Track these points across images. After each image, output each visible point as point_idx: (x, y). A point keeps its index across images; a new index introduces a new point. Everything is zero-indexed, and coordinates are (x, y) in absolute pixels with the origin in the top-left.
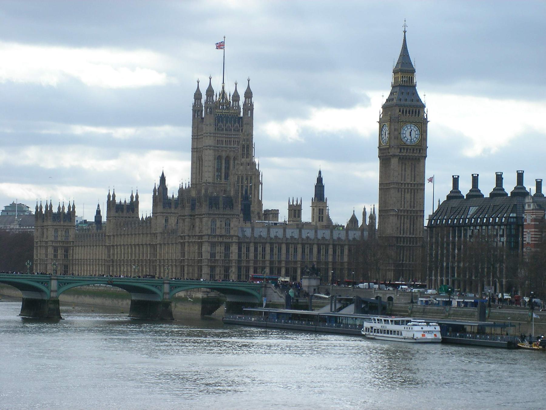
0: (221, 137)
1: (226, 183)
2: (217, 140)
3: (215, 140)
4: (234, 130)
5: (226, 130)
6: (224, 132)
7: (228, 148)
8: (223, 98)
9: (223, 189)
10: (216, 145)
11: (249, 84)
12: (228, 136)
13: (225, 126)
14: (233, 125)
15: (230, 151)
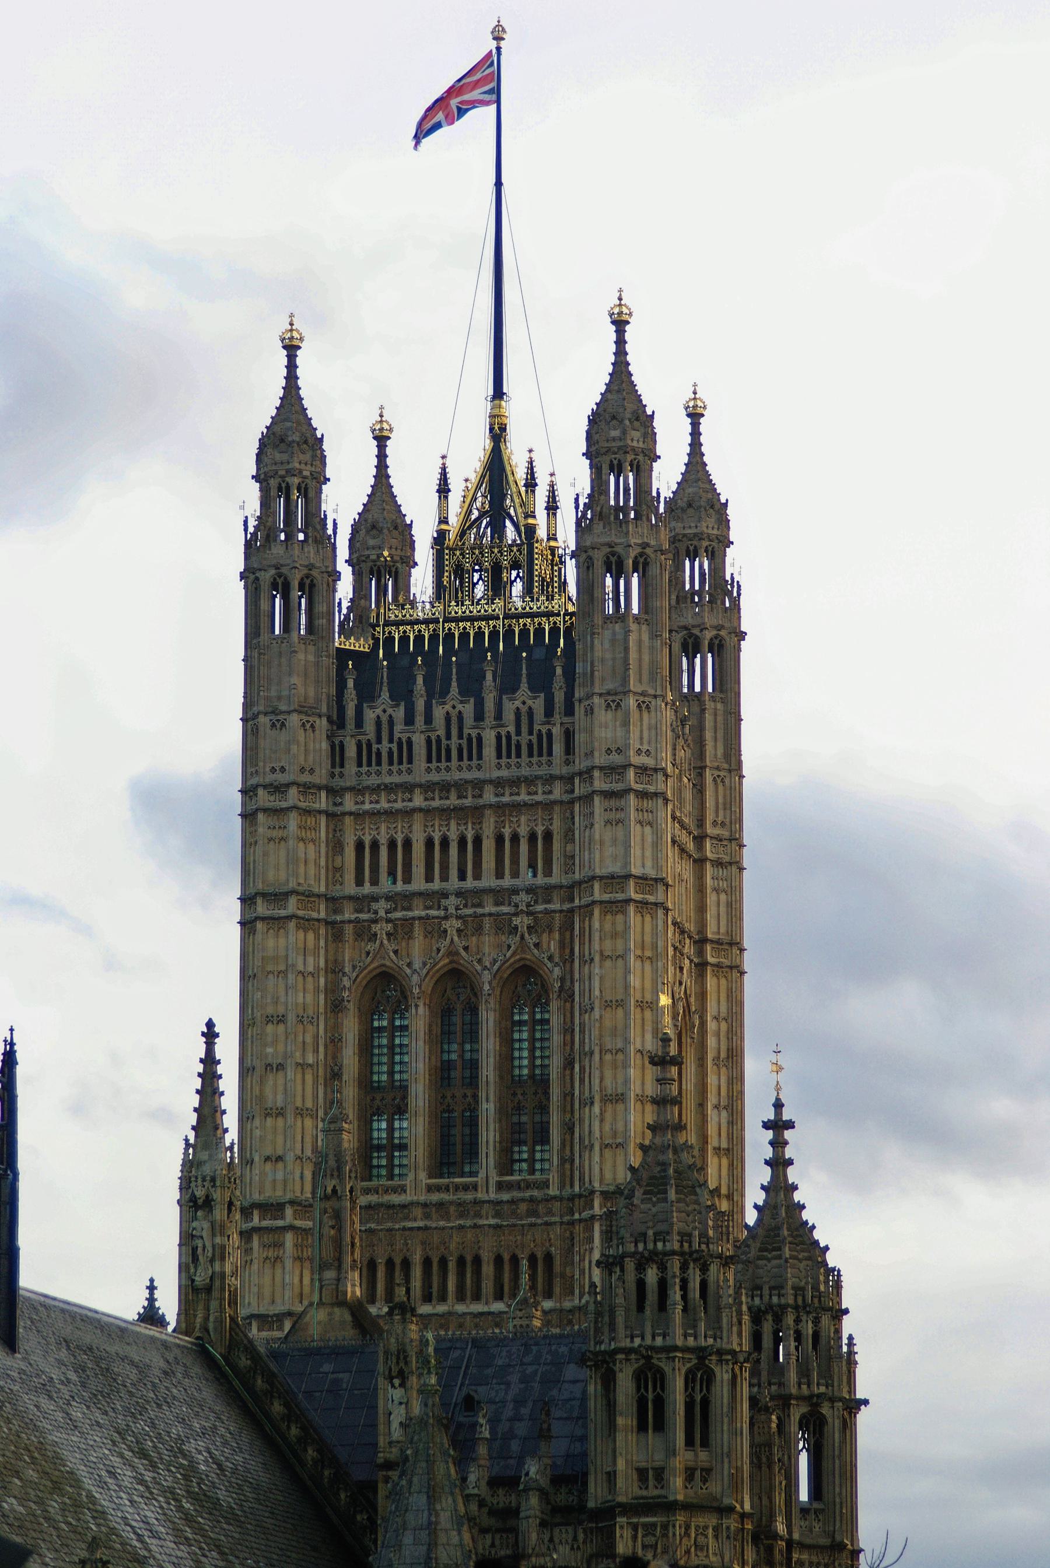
0: (389, 813)
1: (435, 1197)
2: (360, 846)
3: (336, 846)
4: (505, 748)
5: (436, 751)
6: (420, 771)
7: (452, 901)
8: (497, 514)
9: (417, 1258)
10: (350, 888)
11: (621, 352)
12: (453, 801)
13: (420, 719)
14: (489, 705)
15: (473, 926)
